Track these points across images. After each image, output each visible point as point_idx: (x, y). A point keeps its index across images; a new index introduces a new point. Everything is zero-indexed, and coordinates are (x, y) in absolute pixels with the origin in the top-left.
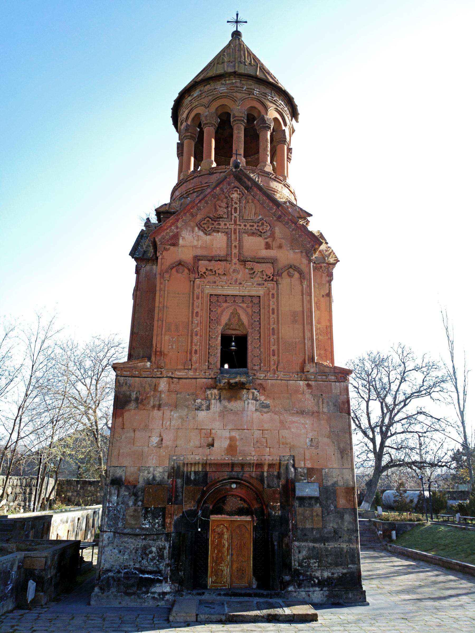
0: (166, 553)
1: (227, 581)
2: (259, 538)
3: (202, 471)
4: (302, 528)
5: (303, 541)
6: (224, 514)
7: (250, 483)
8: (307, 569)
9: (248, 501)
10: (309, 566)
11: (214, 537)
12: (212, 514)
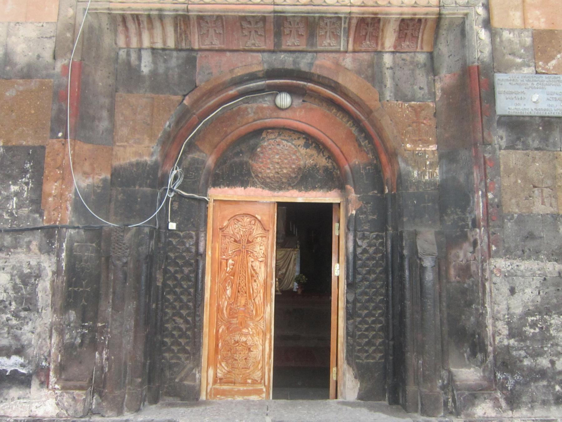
0: (45, 290)
1: (263, 377)
2: (365, 251)
3: (178, 50)
4: (520, 215)
5: (524, 255)
6: (254, 185)
7: (336, 87)
8: (537, 346)
9: (329, 143)
10: (545, 337)
11: (224, 251)
12: (215, 185)
